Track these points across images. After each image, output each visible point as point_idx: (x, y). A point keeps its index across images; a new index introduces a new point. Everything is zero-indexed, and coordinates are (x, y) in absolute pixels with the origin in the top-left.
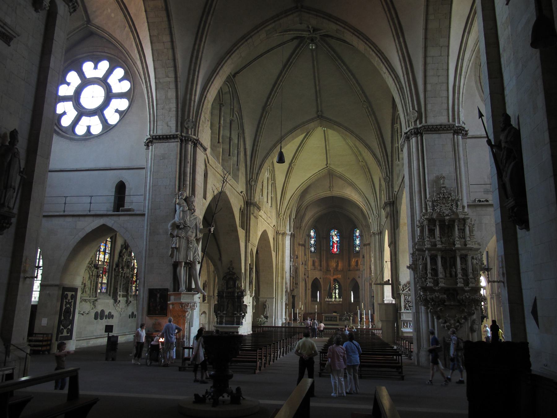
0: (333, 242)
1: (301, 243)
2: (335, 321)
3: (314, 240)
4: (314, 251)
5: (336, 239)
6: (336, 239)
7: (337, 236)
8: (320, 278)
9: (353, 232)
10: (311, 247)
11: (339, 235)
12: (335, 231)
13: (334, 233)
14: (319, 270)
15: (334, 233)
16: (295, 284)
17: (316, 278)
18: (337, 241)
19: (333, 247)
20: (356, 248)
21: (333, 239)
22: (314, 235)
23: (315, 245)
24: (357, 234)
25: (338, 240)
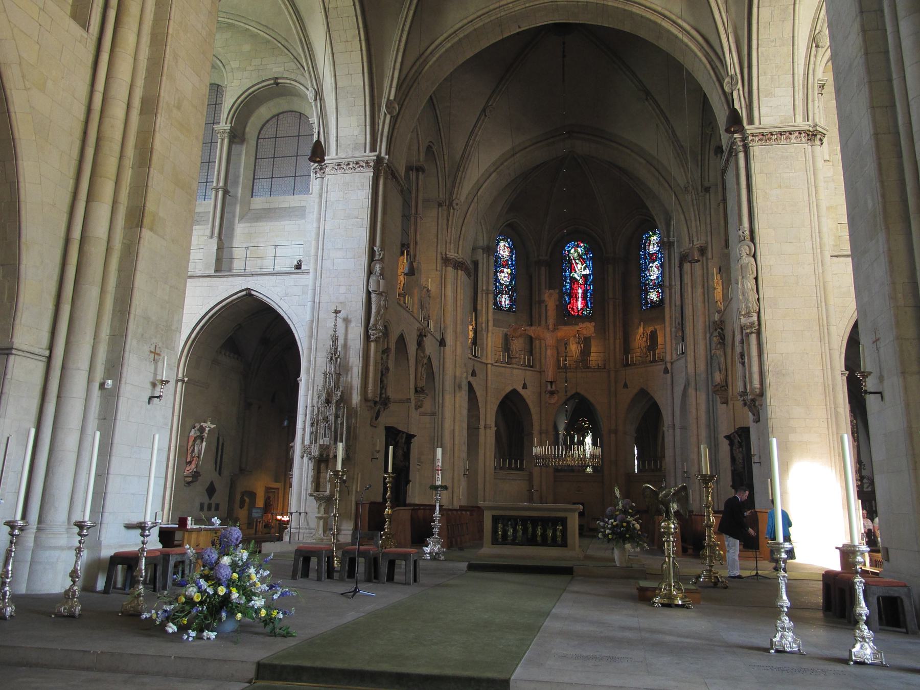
0: (573, 280)
1: (452, 255)
2: (554, 543)
3: (509, 271)
4: (511, 307)
5: (581, 270)
6: (581, 270)
7: (584, 262)
8: (525, 387)
9: (641, 245)
10: (501, 293)
11: (590, 259)
12: (578, 246)
13: (574, 251)
14: (526, 366)
15: (576, 251)
16: (416, 391)
17: (514, 392)
18: (585, 277)
19: (573, 295)
20: (647, 292)
21: (572, 269)
22: (511, 257)
23: (512, 290)
24: (653, 249)
25: (587, 272)
